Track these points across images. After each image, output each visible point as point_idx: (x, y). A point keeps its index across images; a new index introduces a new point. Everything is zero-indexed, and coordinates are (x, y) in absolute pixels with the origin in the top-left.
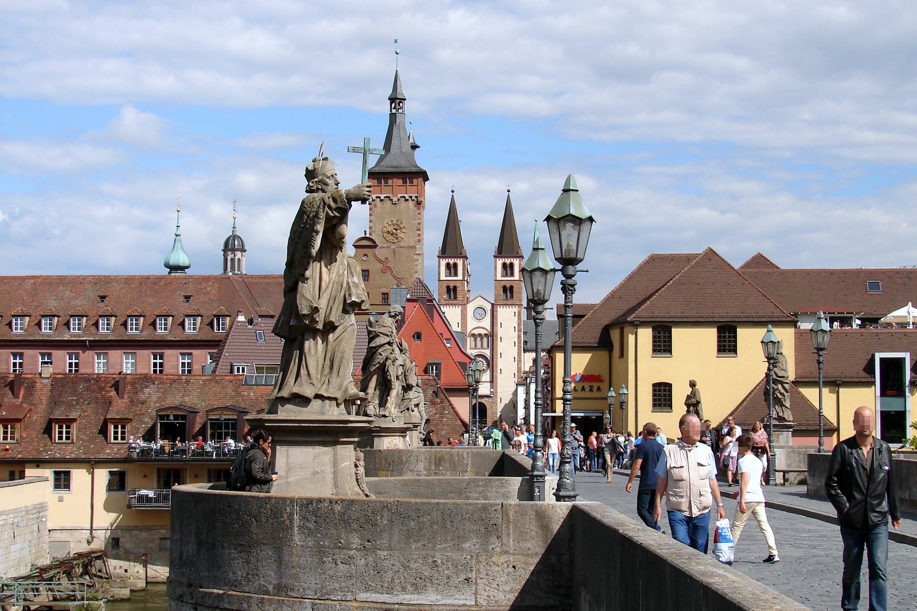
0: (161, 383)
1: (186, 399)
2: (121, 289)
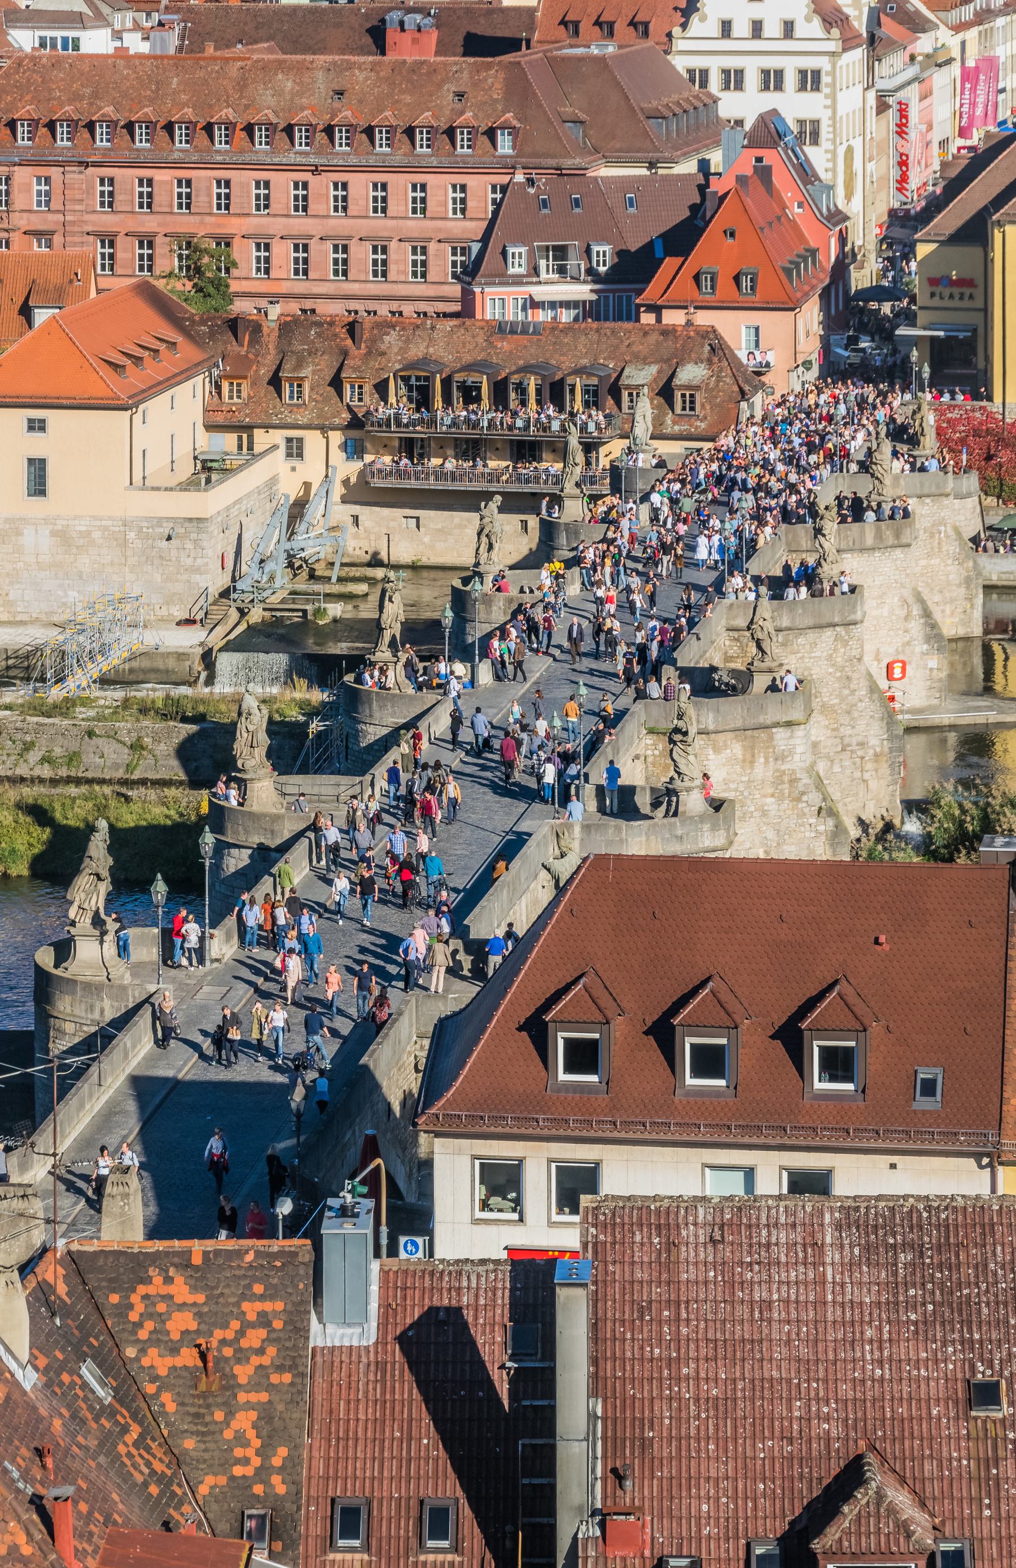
0: (403, 329)
1: (431, 350)
2: (366, 79)
